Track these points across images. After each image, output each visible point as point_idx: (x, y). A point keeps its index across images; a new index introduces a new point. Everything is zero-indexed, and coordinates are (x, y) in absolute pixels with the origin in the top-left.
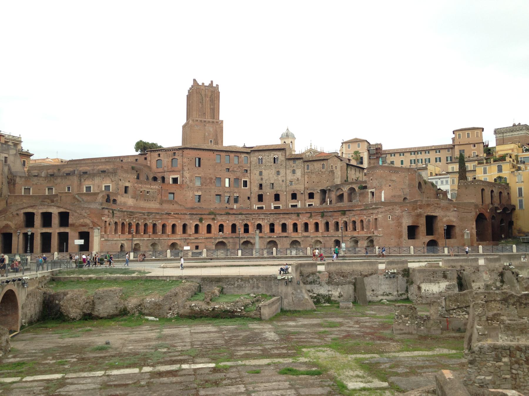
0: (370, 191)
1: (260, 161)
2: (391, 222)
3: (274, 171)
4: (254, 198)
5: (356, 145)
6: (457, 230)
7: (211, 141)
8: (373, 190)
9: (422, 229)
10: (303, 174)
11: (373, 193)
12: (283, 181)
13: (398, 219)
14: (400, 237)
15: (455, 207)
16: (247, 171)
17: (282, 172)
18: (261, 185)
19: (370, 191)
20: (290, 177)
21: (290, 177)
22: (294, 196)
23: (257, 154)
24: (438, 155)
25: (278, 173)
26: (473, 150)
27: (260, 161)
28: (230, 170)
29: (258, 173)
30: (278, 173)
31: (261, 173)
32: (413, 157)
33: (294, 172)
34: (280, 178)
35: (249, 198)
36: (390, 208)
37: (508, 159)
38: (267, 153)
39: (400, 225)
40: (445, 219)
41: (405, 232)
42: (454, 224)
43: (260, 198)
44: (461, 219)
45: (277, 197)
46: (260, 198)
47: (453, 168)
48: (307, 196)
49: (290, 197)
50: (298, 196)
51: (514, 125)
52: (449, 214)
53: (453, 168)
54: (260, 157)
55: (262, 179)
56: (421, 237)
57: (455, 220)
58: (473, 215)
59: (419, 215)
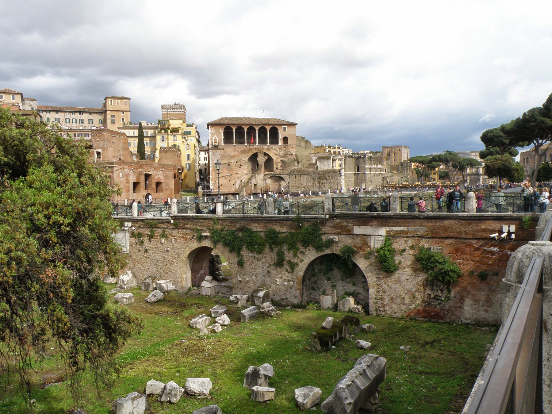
0: (95, 151)
2: (122, 179)
6: (163, 185)
8: (100, 150)
9: (142, 184)
11: (99, 153)
13: (127, 176)
14: (128, 191)
15: (162, 168)
19: (95, 151)
24: (92, 117)
26: (122, 116)
32: (68, 116)
36: (122, 167)
37: (180, 132)
39: (128, 181)
40: (156, 177)
41: (131, 186)
42: (161, 181)
44: (166, 177)
47: (134, 133)
51: (175, 104)
52: (158, 173)
53: (134, 133)
56: (142, 192)
57: (162, 178)
58: (171, 174)
59: (140, 174)
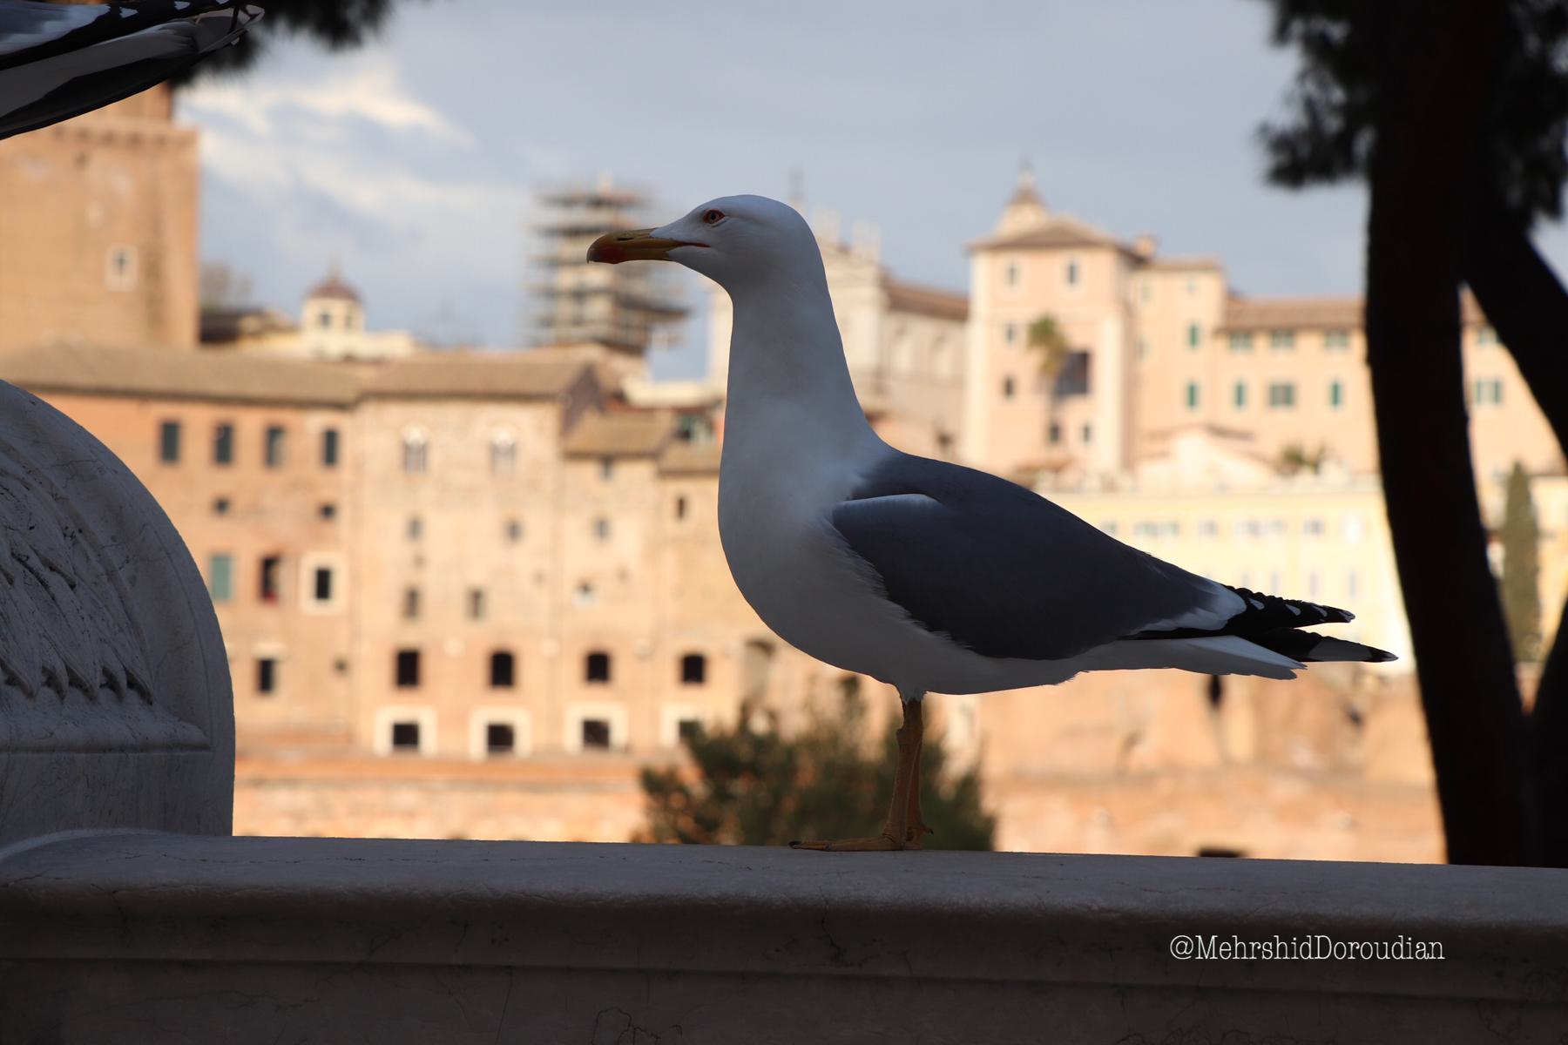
1: (413, 457)
3: (488, 520)
4: (376, 670)
5: (1053, 265)
7: (121, 262)
10: (653, 550)
12: (539, 578)
16: (328, 511)
17: (537, 523)
18: (412, 602)
20: (581, 555)
21: (581, 555)
22: (598, 667)
23: (394, 413)
25: (514, 531)
27: (413, 457)
28: (240, 503)
29: (396, 524)
30: (514, 531)
31: (415, 528)
33: (601, 528)
34: (524, 558)
35: (341, 667)
38: (453, 413)
43: (408, 668)
45: (502, 669)
46: (408, 668)
48: (670, 671)
49: (574, 668)
50: (621, 669)
54: (415, 435)
55: (419, 562)
